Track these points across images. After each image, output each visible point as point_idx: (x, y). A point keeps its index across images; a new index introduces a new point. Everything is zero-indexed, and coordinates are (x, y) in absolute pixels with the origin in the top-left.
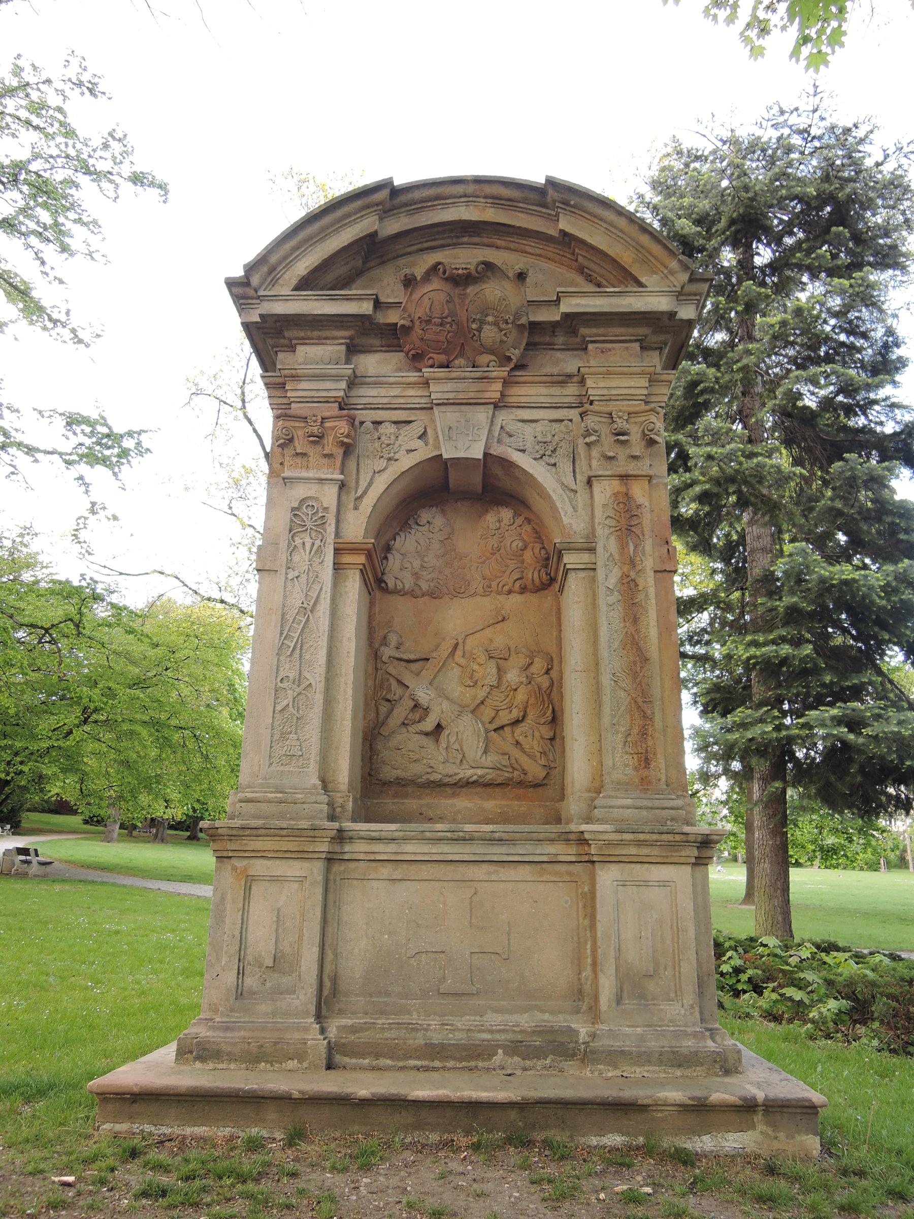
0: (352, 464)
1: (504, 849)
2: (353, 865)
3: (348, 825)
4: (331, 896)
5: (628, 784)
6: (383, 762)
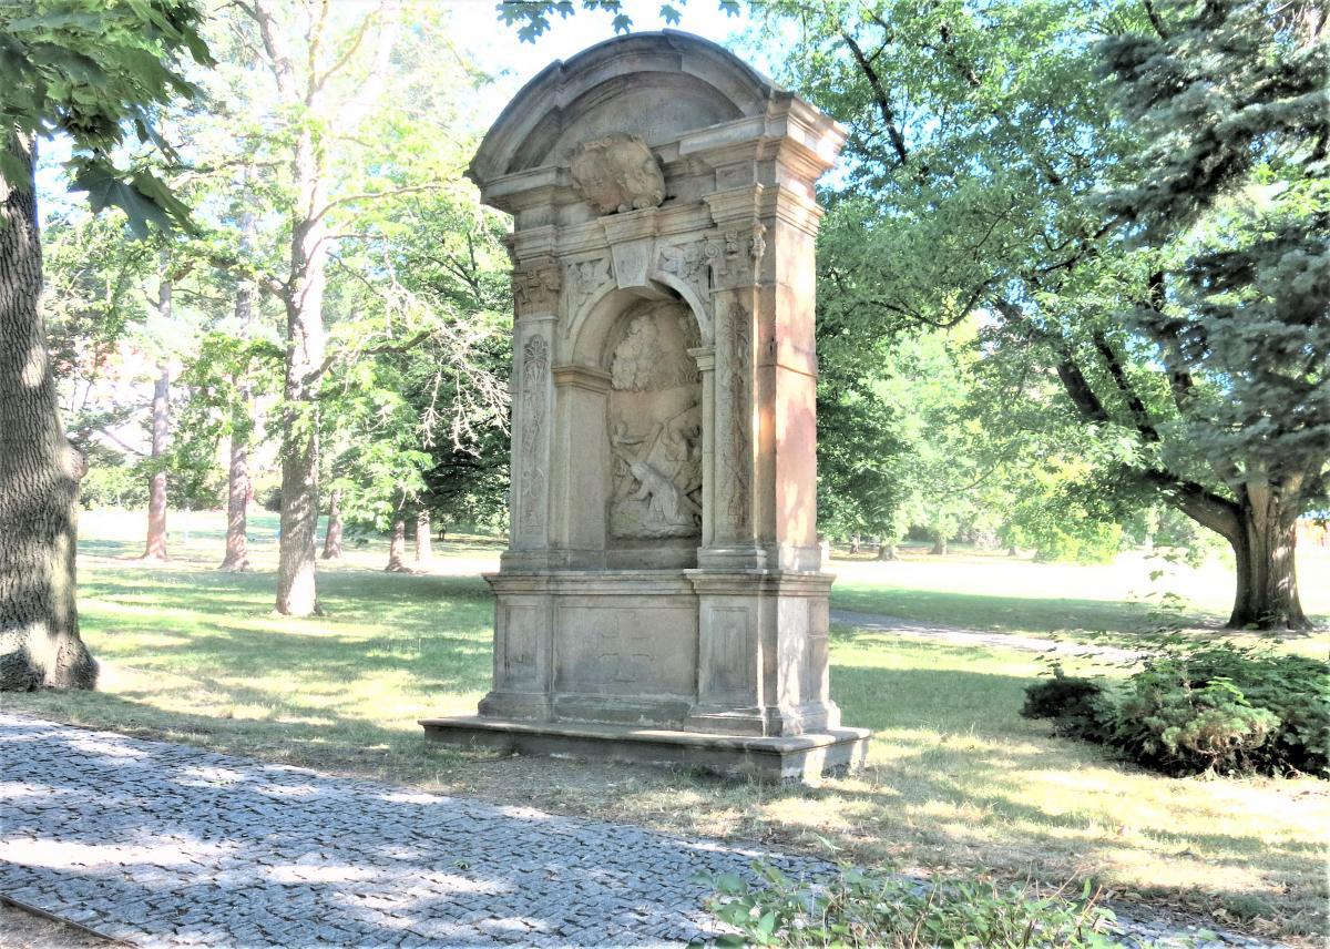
0: (563, 301)
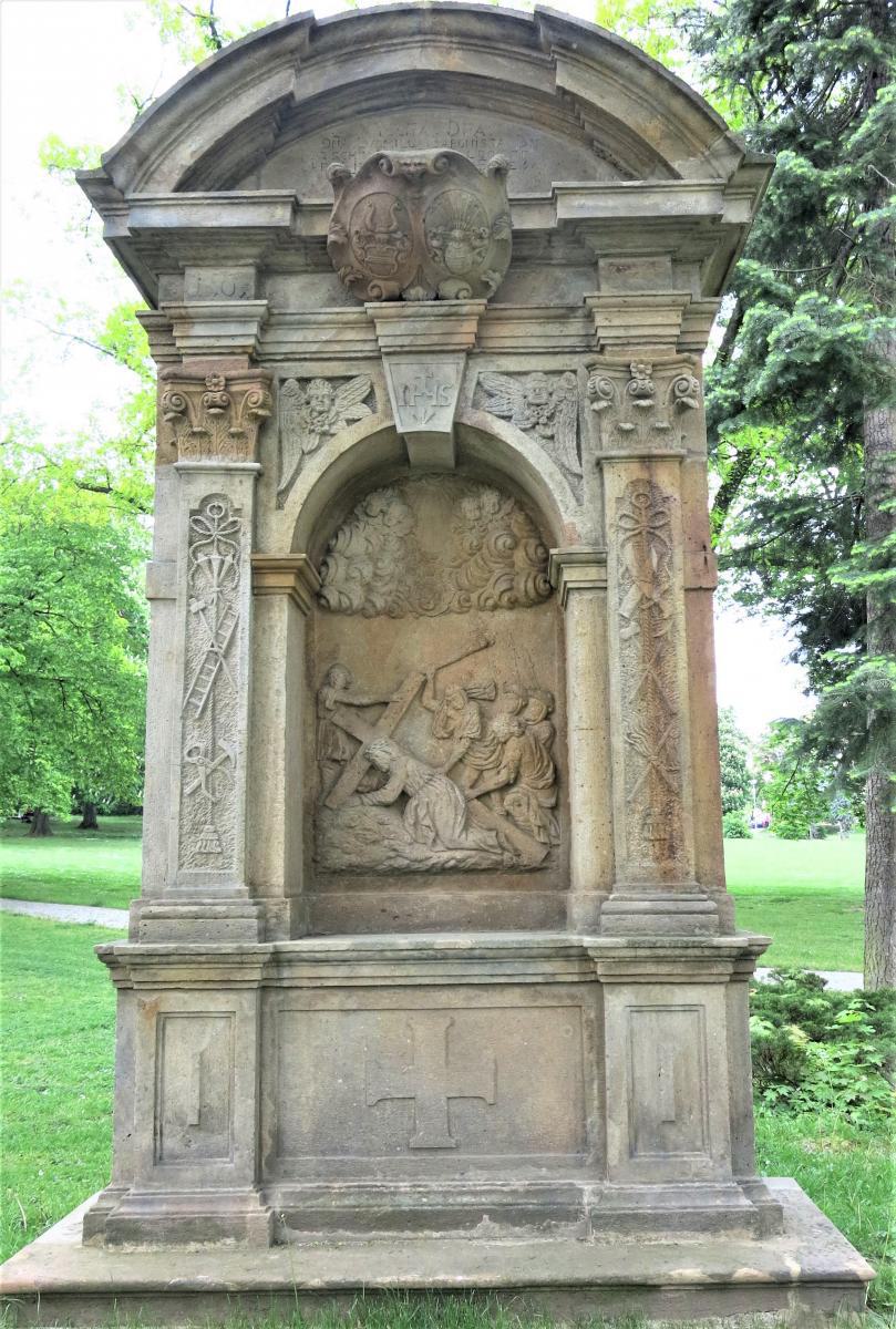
0: (271, 443)
1: (487, 969)
2: (293, 994)
3: (287, 944)
4: (268, 1034)
5: (645, 880)
6: (332, 845)
